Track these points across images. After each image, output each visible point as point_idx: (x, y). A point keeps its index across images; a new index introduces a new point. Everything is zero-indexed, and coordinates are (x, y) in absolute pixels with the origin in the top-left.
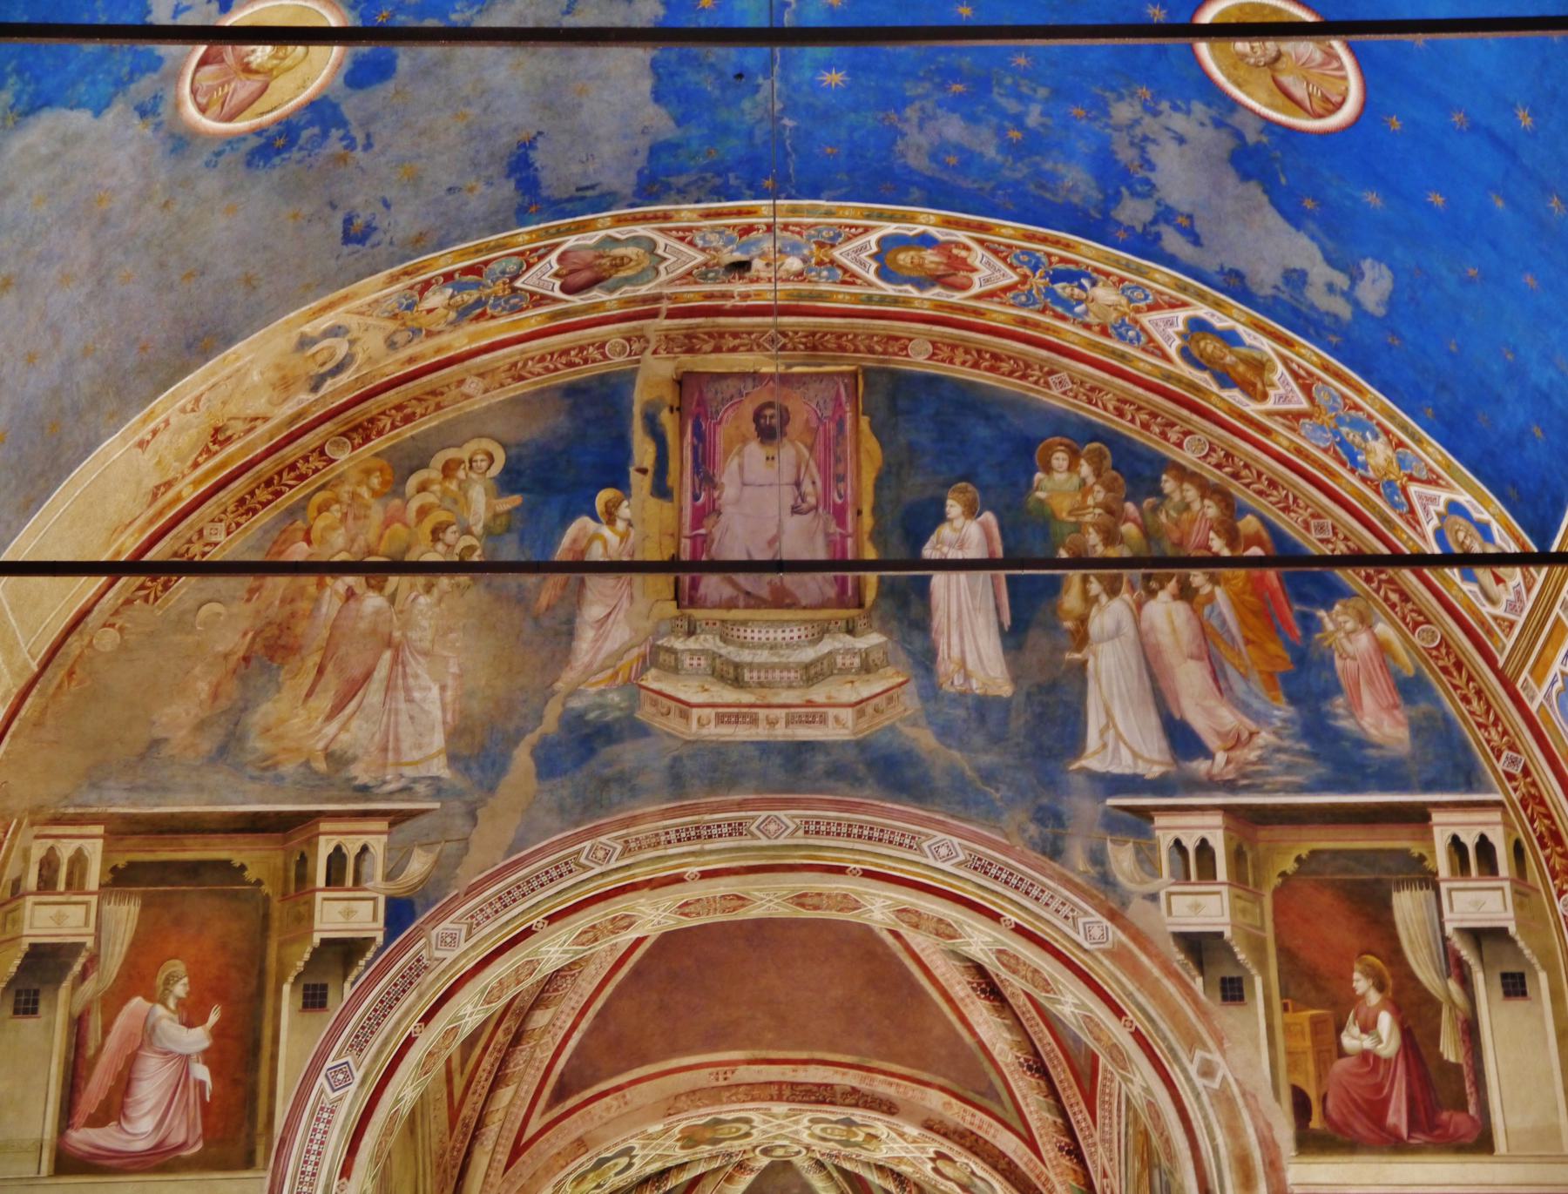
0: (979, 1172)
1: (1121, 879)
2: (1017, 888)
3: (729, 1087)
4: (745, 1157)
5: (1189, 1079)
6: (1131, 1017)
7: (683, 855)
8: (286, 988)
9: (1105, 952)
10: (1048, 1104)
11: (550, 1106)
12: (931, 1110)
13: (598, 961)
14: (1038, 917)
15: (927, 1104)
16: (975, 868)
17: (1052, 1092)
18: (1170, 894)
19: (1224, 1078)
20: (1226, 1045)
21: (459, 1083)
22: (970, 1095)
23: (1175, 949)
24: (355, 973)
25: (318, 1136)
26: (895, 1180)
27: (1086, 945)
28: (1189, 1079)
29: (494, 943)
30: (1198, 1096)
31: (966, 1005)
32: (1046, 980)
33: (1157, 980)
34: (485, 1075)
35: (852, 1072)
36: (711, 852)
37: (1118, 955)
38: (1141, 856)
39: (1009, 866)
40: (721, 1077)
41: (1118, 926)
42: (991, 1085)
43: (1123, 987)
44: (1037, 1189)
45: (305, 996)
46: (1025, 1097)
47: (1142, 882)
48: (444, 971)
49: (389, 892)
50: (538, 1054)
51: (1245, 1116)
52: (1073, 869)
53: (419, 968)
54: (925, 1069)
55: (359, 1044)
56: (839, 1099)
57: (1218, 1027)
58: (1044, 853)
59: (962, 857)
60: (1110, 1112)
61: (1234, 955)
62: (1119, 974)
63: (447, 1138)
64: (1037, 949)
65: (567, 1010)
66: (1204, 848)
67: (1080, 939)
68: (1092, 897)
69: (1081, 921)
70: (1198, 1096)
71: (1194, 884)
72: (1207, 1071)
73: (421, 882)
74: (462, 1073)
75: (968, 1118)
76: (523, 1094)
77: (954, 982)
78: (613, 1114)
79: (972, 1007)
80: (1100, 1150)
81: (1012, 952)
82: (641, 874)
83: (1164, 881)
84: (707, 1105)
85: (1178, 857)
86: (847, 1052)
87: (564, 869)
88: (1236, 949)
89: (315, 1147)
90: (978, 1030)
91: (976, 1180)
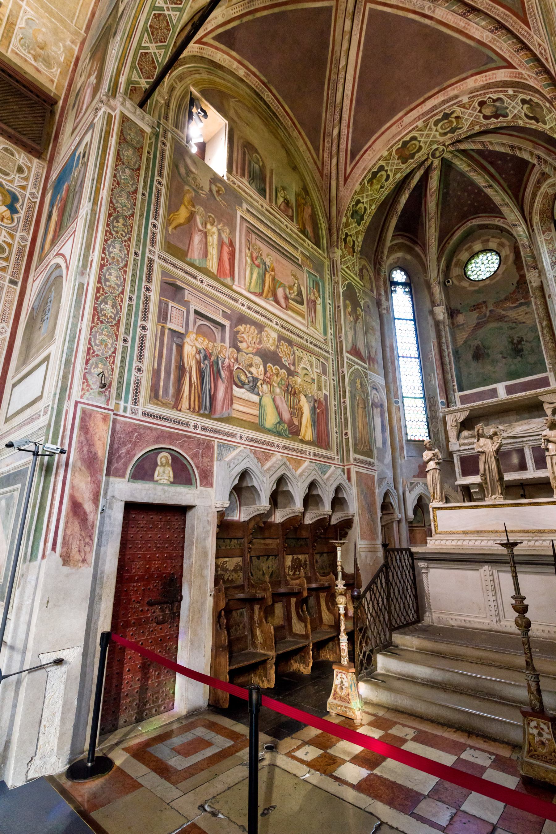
0: (495, 96)
11: (351, 162)
15: (469, 87)
35: (439, 95)
42: (488, 56)
46: (501, 49)
60: (535, 15)
75: (484, 79)
78: (371, 156)
79: (469, 27)
80: (535, 37)
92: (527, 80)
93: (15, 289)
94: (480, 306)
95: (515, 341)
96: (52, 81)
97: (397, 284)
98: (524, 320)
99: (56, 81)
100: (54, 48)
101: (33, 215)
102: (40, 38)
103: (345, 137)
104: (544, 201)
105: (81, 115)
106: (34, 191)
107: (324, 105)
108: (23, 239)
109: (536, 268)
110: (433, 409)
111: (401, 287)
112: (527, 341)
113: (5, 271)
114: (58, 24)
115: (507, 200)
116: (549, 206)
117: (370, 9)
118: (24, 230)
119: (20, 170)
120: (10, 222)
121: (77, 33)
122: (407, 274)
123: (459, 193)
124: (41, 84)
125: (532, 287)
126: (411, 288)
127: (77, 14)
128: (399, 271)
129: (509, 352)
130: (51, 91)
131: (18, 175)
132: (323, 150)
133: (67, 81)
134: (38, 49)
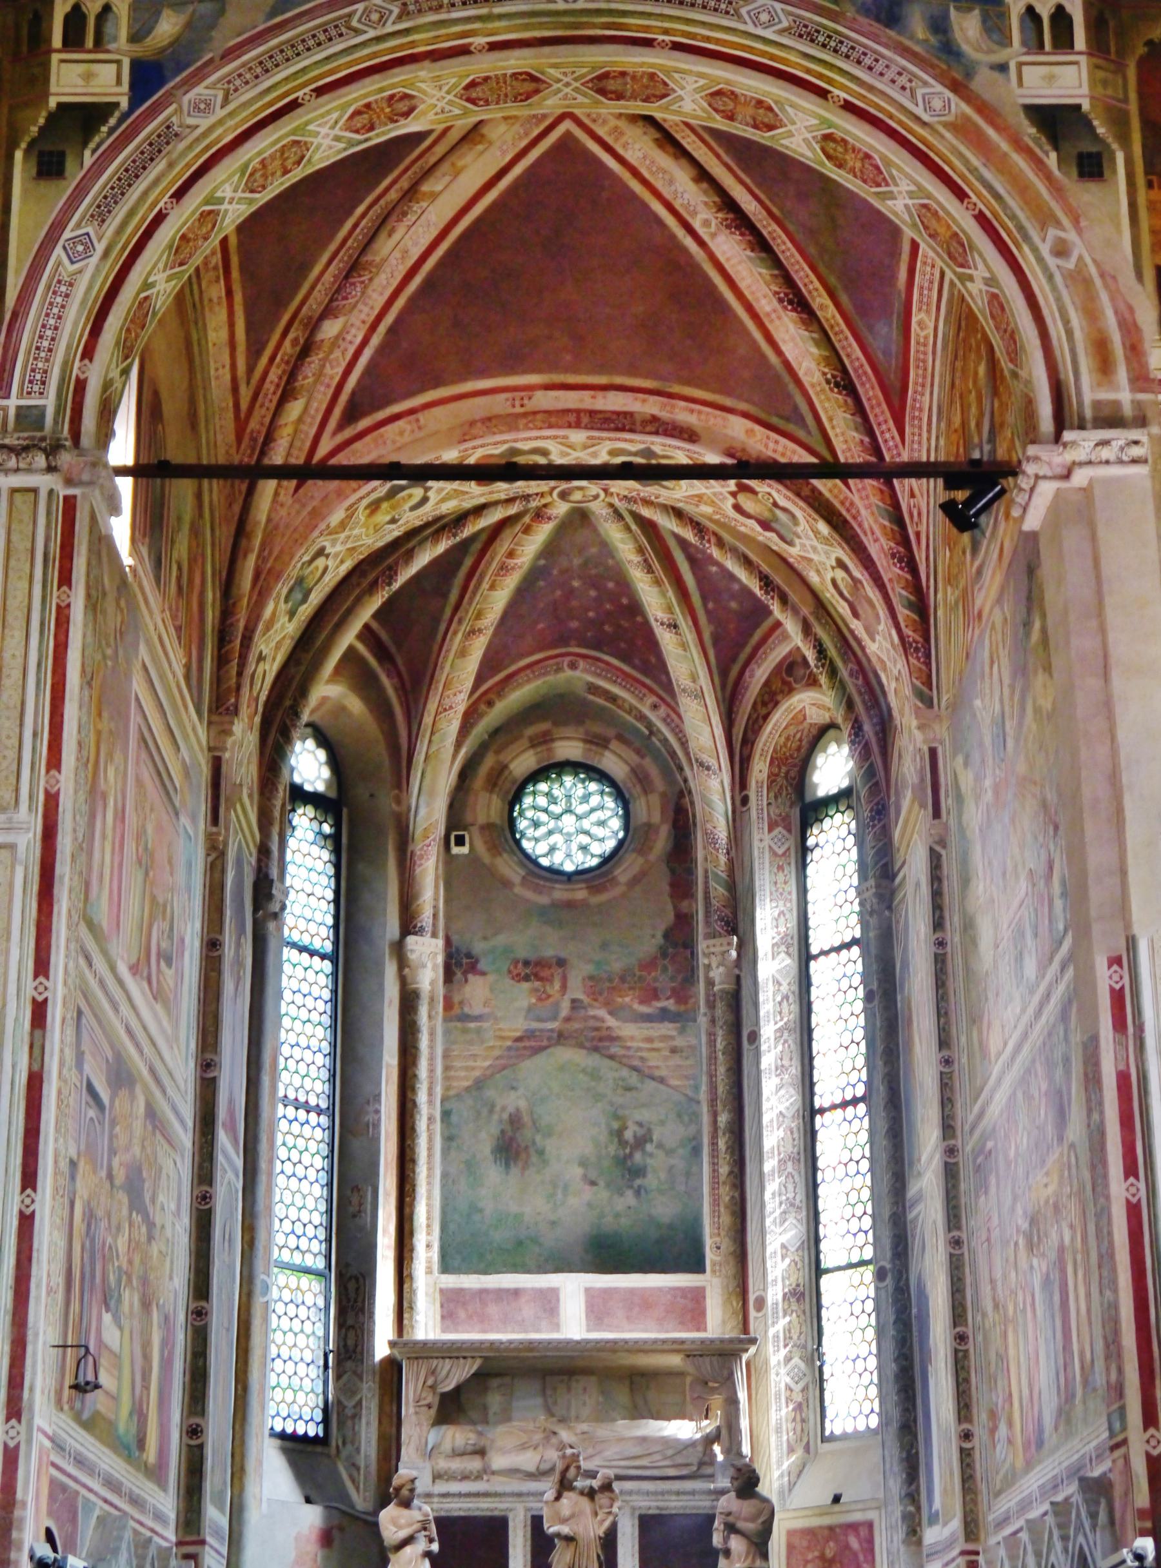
0: (782, 502)
1: (966, 48)
2: (847, 57)
3: (525, 415)
4: (544, 501)
5: (1040, 259)
6: (974, 198)
7: (468, 20)
8: (19, 155)
9: (946, 125)
10: (855, 422)
11: (340, 427)
12: (733, 438)
13: (388, 270)
14: (871, 88)
15: (729, 432)
16: (801, 36)
17: (860, 410)
18: (1020, 65)
19: (1080, 258)
20: (1083, 224)
21: (245, 394)
22: (775, 420)
23: (1026, 123)
24: (97, 139)
25: (55, 310)
26: (693, 528)
27: (926, 117)
28: (1040, 259)
29: (255, 114)
30: (1050, 278)
31: (772, 321)
32: (877, 168)
33: (1005, 155)
34: (272, 389)
35: (652, 399)
36: (501, 17)
37: (961, 128)
38: (989, 23)
39: (836, 32)
40: (517, 403)
41: (962, 98)
42: (796, 408)
43: (966, 162)
44: (841, 515)
45: (40, 164)
46: (831, 419)
47: (990, 51)
48: (197, 140)
49: (135, 55)
50: (328, 370)
51: (1104, 297)
52: (912, 38)
53: (168, 135)
54: (728, 393)
55: (100, 215)
56: (638, 427)
57: (1074, 204)
58: (878, 20)
59: (785, 24)
60: (920, 428)
61: (1092, 129)
62: (963, 149)
63: (233, 451)
64: (867, 127)
65: (358, 323)
66: (1061, 16)
67: (919, 111)
68: (933, 66)
69: (920, 92)
70: (1050, 278)
71: (1048, 54)
72: (1061, 250)
73: (171, 44)
74: (248, 383)
75: (771, 445)
76: (312, 412)
77: (759, 295)
78: (407, 438)
79: (777, 322)
81: (839, 134)
82: (422, 41)
83: (1015, 51)
84: (502, 432)
85: (1030, 24)
86: (646, 376)
87: (333, 33)
88: (1096, 123)
89: (52, 322)
90: (787, 349)
91: (778, 512)
92: (865, 534)
94: (545, 973)
95: (628, 1135)
97: (299, 795)
98: (663, 1073)
103: (351, 350)
104: (792, 730)
107: (333, 247)
109: (734, 931)
110: (350, 1322)
111: (310, 811)
112: (660, 1146)
115: (704, 681)
116: (799, 749)
117: (568, 134)
122: (334, 762)
123: (576, 584)
125: (710, 983)
126: (337, 825)
128: (310, 744)
129: (606, 1163)
132: (272, 359)
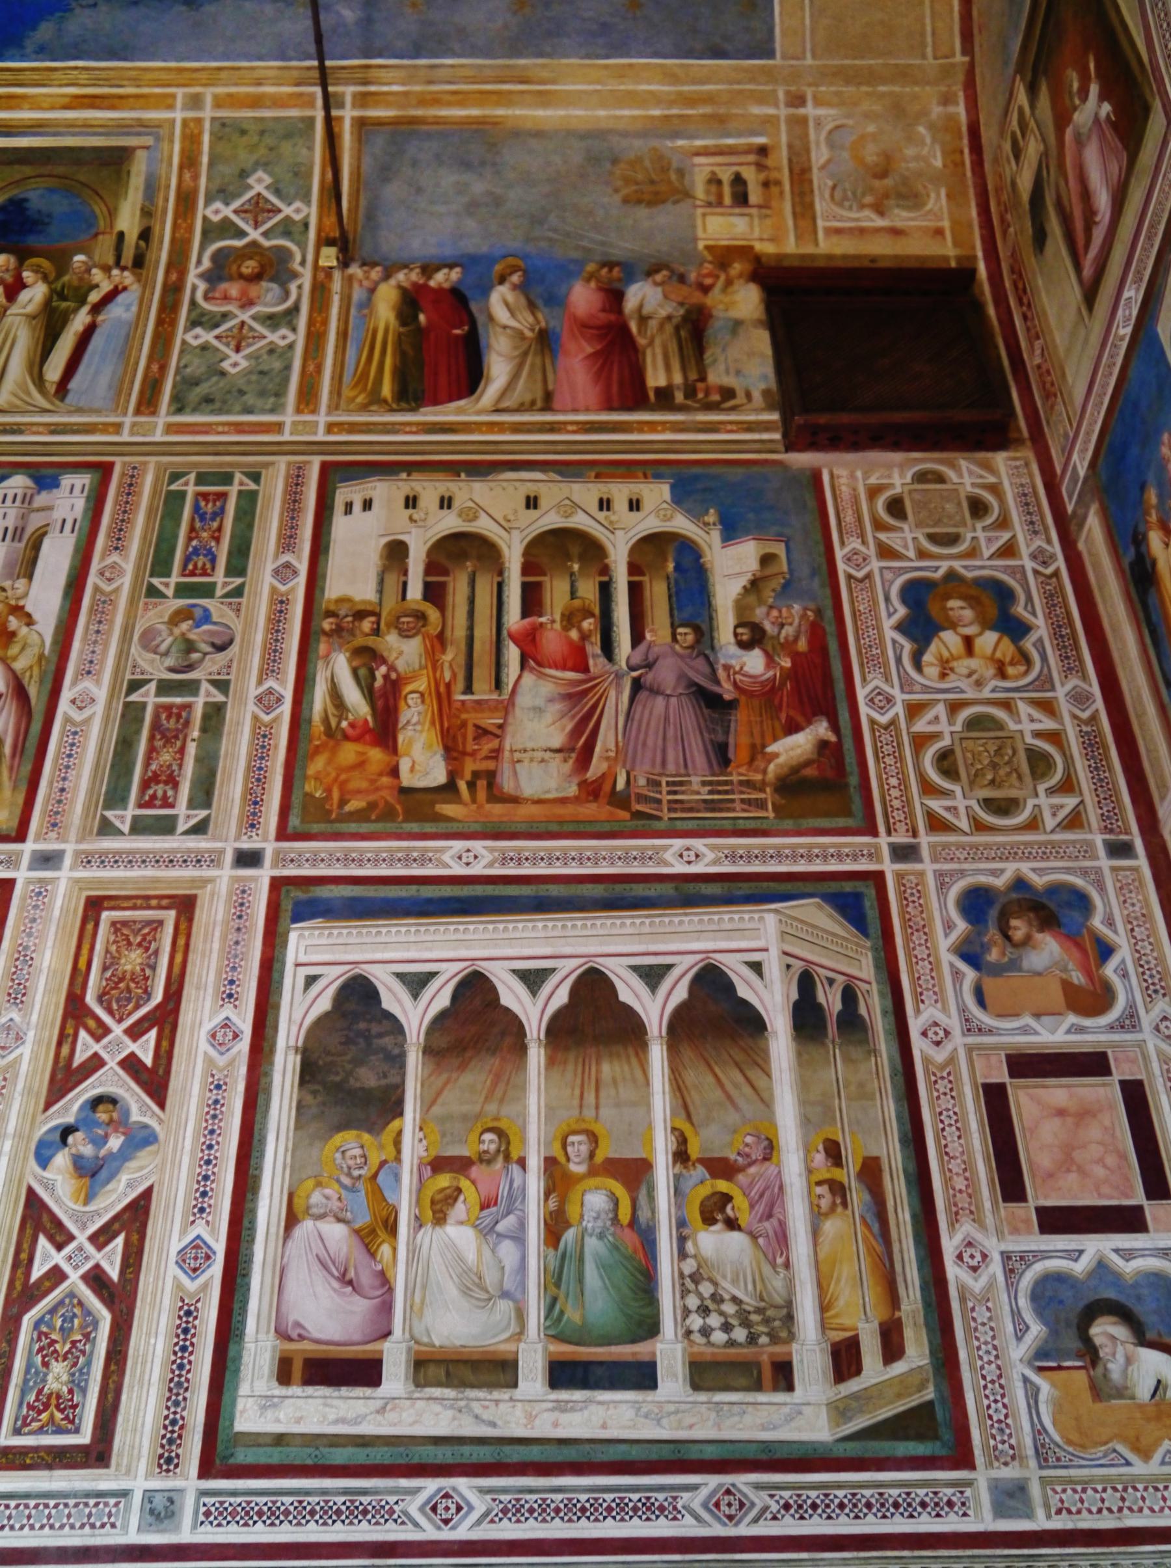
93: (1135, 869)
96: (939, 232)
99: (946, 224)
100: (910, 152)
101: (1069, 614)
102: (871, 154)
105: (1098, 235)
106: (1039, 542)
108: (1080, 698)
113: (1081, 826)
114: (897, 89)
118: (1068, 671)
119: (978, 508)
120: (1022, 668)
121: (946, 72)
124: (918, 258)
127: (929, 29)
130: (946, 259)
131: (979, 525)
133: (973, 204)
134: (877, 183)
